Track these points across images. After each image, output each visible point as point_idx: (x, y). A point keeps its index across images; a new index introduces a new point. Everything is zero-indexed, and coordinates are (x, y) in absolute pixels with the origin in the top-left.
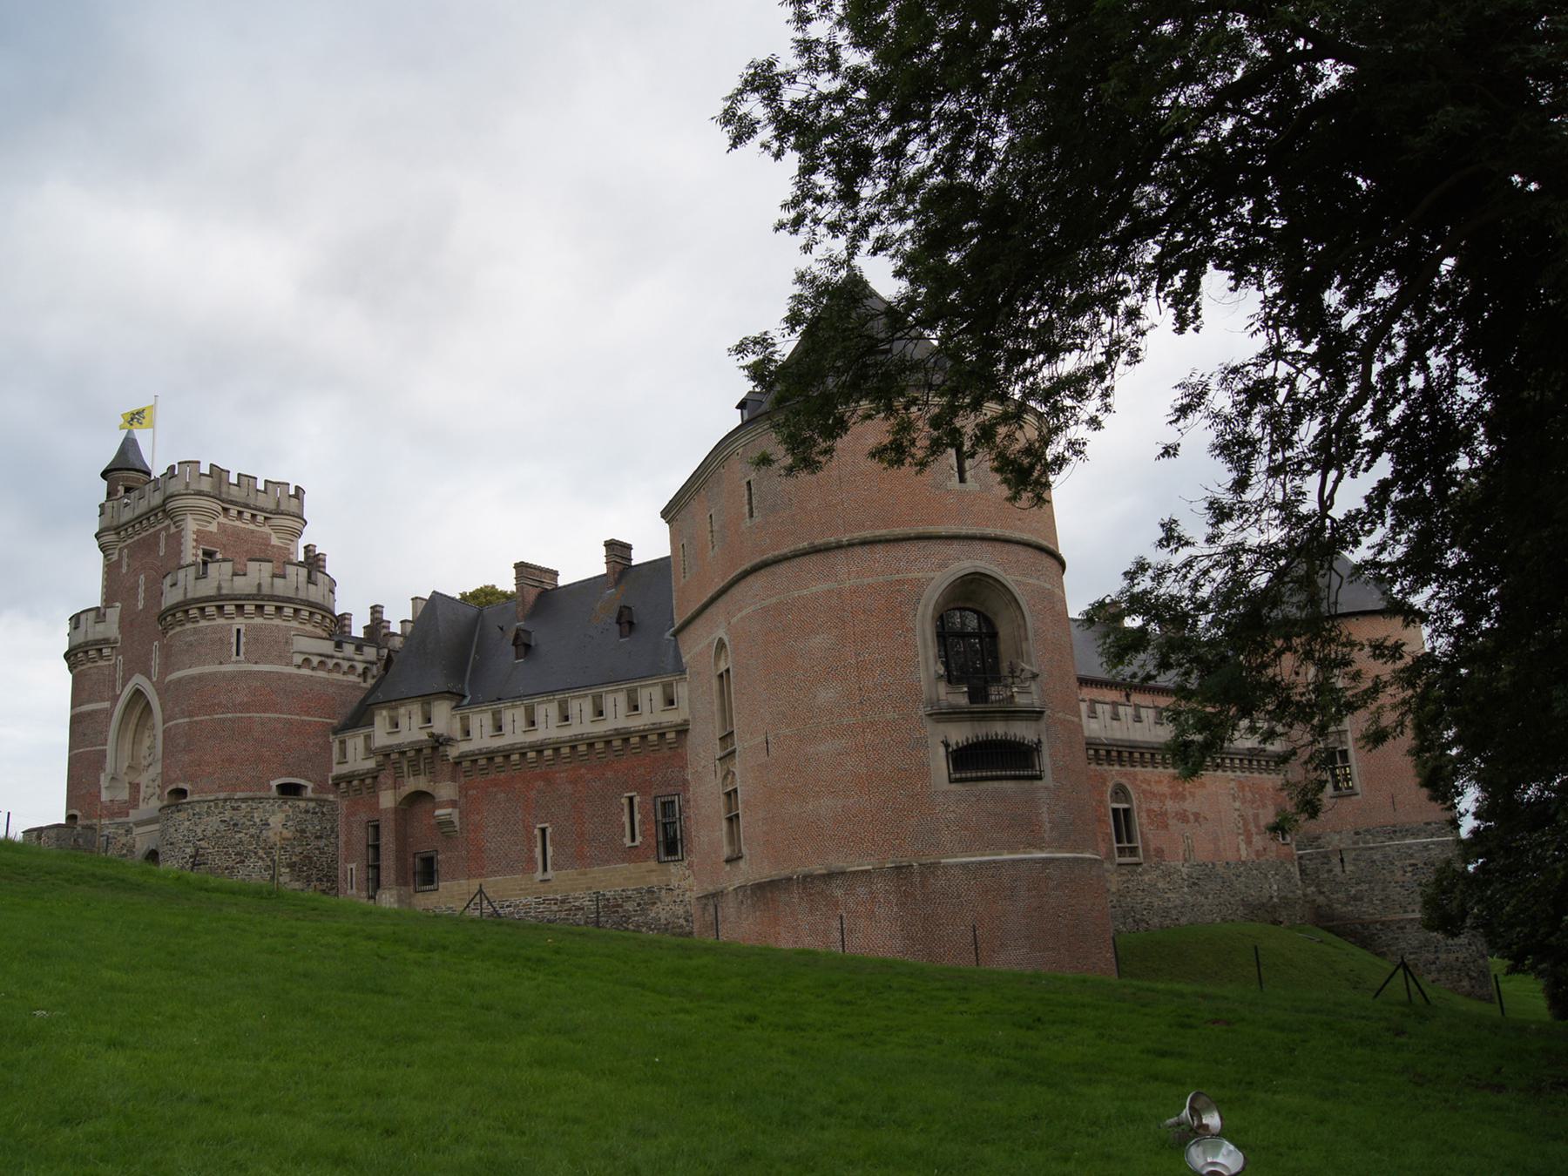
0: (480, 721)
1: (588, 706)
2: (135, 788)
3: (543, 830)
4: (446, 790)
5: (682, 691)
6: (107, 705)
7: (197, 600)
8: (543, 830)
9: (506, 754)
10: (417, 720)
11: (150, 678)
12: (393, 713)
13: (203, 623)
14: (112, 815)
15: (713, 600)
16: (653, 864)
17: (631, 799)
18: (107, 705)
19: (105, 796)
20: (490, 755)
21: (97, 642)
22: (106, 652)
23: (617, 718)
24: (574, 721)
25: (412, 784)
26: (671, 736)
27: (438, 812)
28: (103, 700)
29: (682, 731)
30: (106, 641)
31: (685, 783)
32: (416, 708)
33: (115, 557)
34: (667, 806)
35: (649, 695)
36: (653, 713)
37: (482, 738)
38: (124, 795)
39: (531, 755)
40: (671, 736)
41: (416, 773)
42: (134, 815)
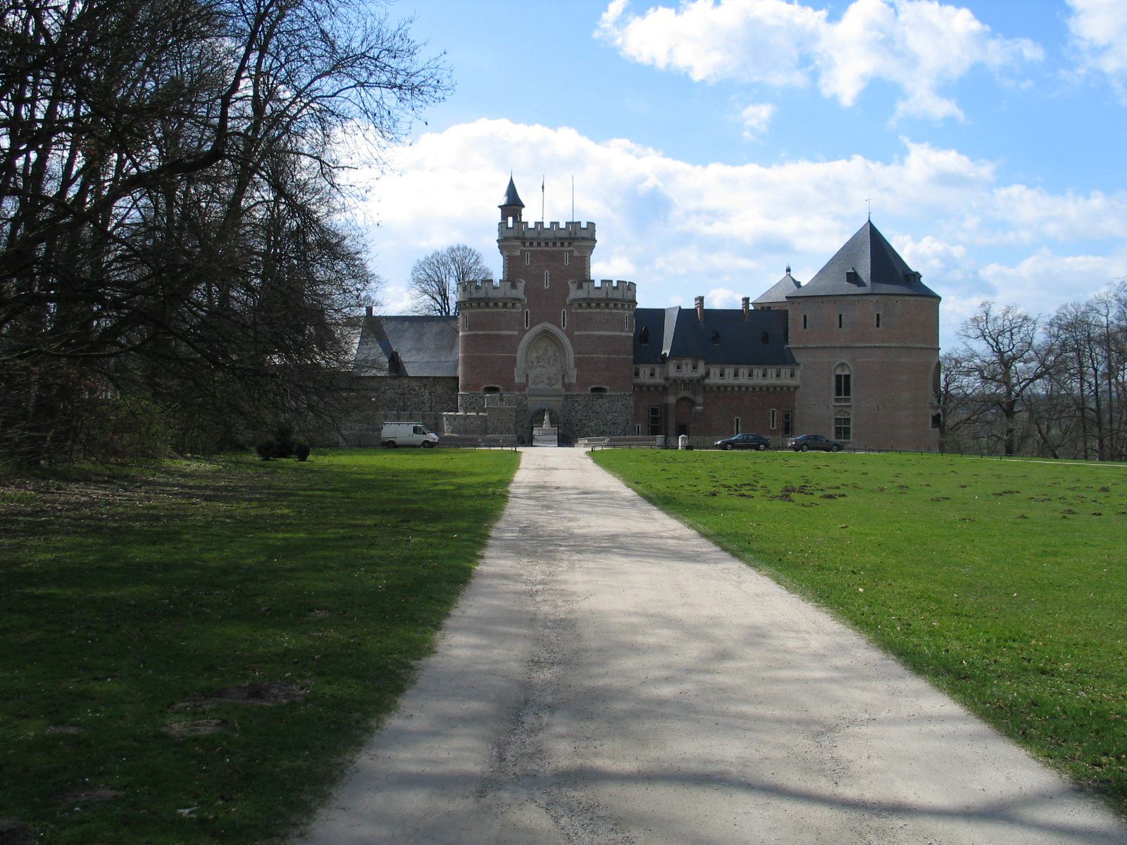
0: (715, 371)
1: (761, 374)
2: (527, 376)
3: (737, 420)
4: (700, 399)
5: (798, 373)
6: (516, 333)
7: (617, 300)
8: (737, 420)
9: (726, 387)
10: (690, 367)
11: (559, 326)
12: (679, 362)
13: (614, 311)
15: (841, 348)
16: (780, 437)
17: (773, 411)
18: (516, 333)
19: (517, 380)
20: (719, 387)
21: (514, 299)
22: (518, 305)
23: (771, 380)
24: (755, 377)
25: (683, 394)
26: (792, 389)
27: (697, 408)
28: (514, 330)
29: (796, 388)
30: (519, 300)
31: (794, 408)
32: (689, 362)
33: (518, 253)
34: (787, 416)
35: (785, 371)
36: (785, 380)
37: (714, 379)
39: (736, 388)
40: (792, 389)
41: (685, 390)
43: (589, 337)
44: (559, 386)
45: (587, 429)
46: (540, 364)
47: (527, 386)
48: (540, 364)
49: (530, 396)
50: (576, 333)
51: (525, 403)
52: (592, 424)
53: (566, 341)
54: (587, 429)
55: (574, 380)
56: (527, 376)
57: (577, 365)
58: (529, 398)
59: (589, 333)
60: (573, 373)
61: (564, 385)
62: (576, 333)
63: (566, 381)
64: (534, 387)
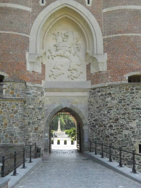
2: (43, 66)
11: (83, 3)
14: (34, 81)
18: (29, 9)
19: (29, 68)
38: (39, 70)
42: (43, 84)
43: (122, 12)
44: (82, 78)
45: (125, 132)
46: (59, 52)
47: (44, 79)
48: (59, 52)
49: (47, 90)
50: (105, 11)
51: (41, 98)
52: (133, 124)
53: (92, 20)
54: (125, 132)
55: (103, 68)
56: (43, 66)
57: (106, 49)
58: (45, 94)
59: (123, 7)
60: (103, 59)
61: (89, 76)
62: (105, 11)
63: (93, 71)
64: (52, 79)
